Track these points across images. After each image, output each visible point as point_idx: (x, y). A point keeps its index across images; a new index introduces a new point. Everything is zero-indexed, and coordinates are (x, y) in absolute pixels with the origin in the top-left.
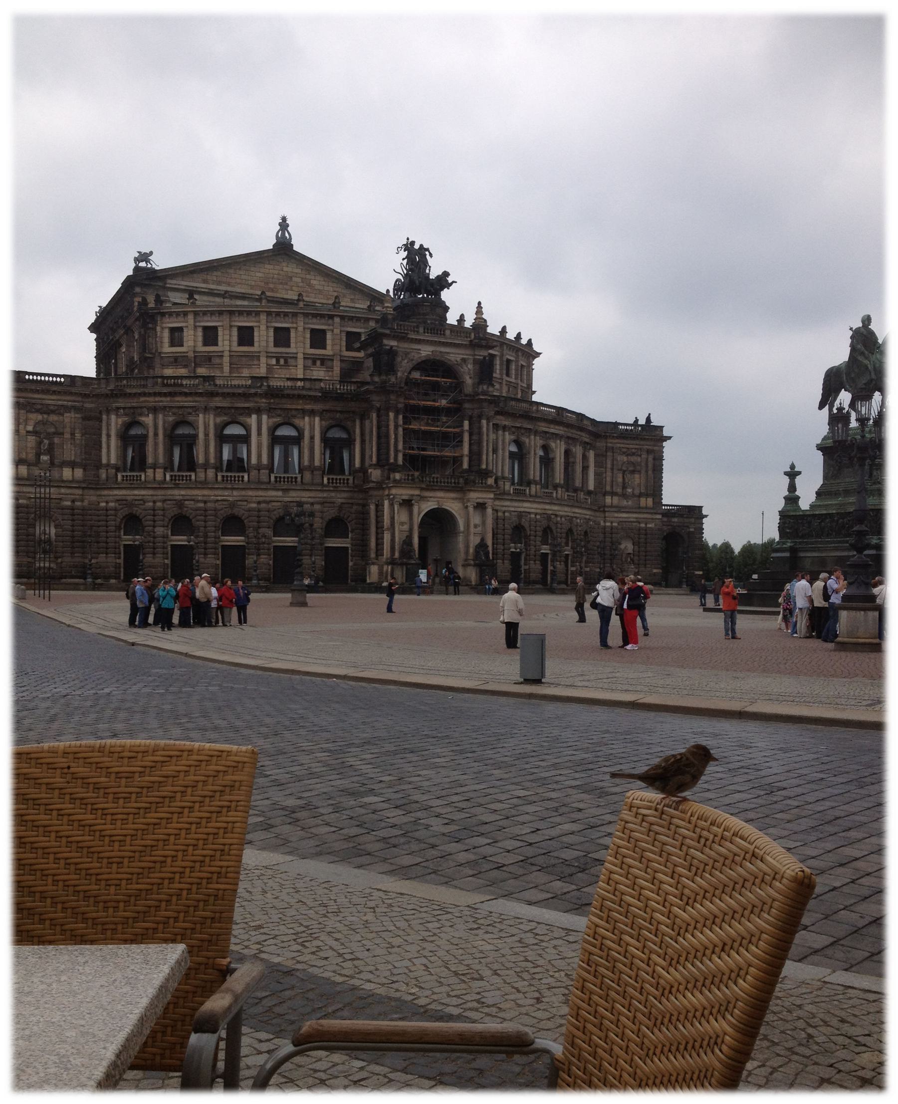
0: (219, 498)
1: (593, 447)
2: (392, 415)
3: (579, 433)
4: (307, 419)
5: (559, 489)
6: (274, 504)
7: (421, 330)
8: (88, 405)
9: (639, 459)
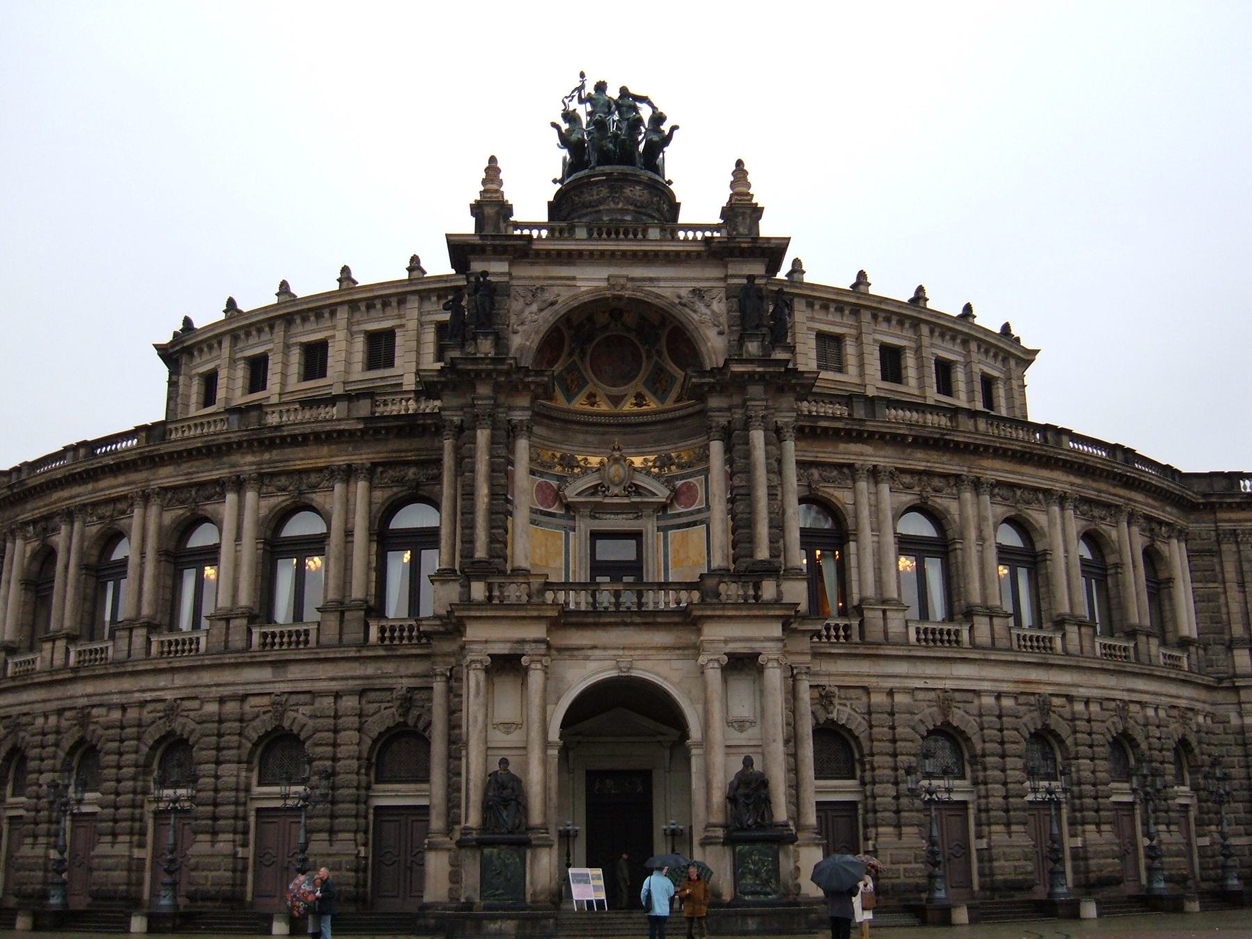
0: (148, 696)
1: (1183, 535)
2: (483, 436)
3: (1122, 492)
4: (339, 488)
5: (1072, 631)
6: (253, 701)
7: (581, 233)
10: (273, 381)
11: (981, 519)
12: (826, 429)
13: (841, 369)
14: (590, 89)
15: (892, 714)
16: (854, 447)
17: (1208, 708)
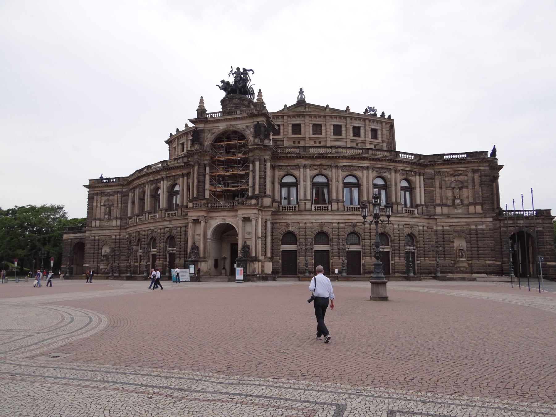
4: (181, 179)
6: (166, 229)
8: (124, 190)
9: (466, 178)
10: (185, 149)
11: (338, 176)
12: (290, 157)
13: (321, 134)
14: (235, 70)
15: (306, 229)
16: (299, 160)
17: (425, 224)
